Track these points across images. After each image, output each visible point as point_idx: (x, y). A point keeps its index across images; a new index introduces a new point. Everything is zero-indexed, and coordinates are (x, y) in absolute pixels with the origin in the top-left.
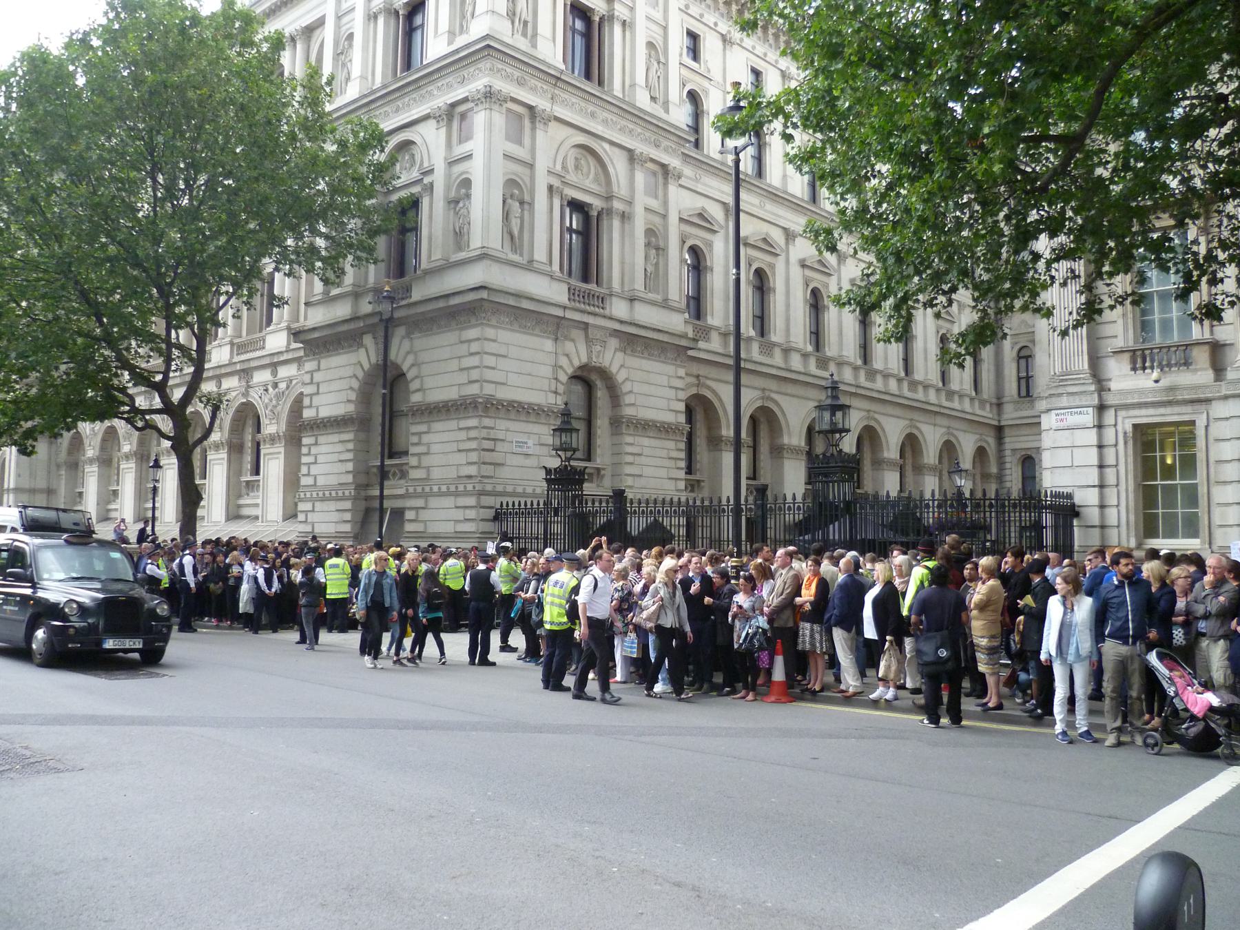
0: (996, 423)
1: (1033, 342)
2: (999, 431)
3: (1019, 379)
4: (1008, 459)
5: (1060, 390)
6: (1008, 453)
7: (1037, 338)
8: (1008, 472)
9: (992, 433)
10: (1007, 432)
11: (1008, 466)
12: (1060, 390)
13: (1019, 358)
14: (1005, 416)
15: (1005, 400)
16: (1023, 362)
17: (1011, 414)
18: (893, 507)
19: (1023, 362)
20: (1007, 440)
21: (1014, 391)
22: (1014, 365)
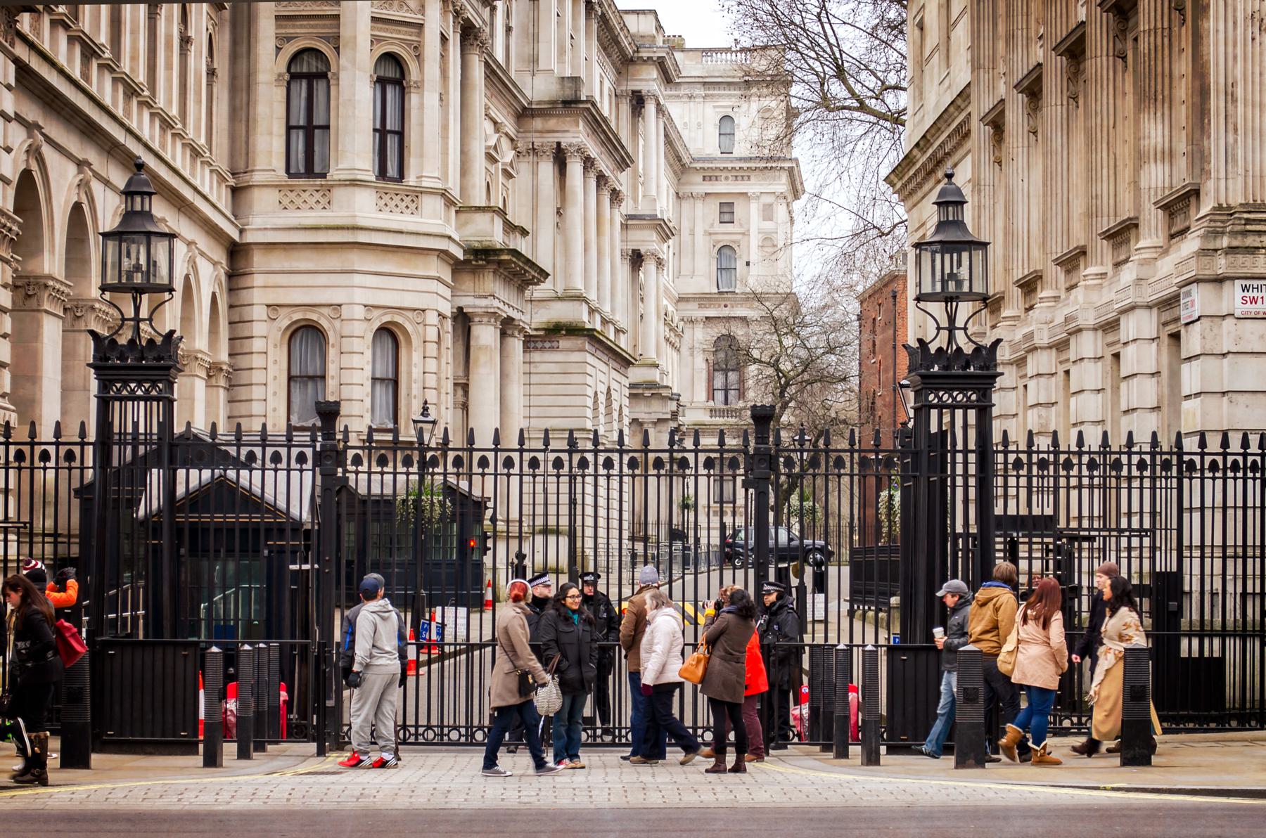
0: (235, 235)
1: (335, 41)
2: (237, 253)
3: (289, 128)
4: (258, 329)
5: (1251, 241)
6: (259, 312)
7: (345, 32)
8: (257, 361)
9: (220, 255)
10: (259, 260)
11: (257, 345)
12: (1251, 241)
13: (294, 77)
14: (256, 221)
15: (258, 178)
16: (301, 89)
17: (268, 217)
18: (135, 444)
19: (301, 89)
20: (258, 280)
21: (280, 164)
22: (280, 93)
